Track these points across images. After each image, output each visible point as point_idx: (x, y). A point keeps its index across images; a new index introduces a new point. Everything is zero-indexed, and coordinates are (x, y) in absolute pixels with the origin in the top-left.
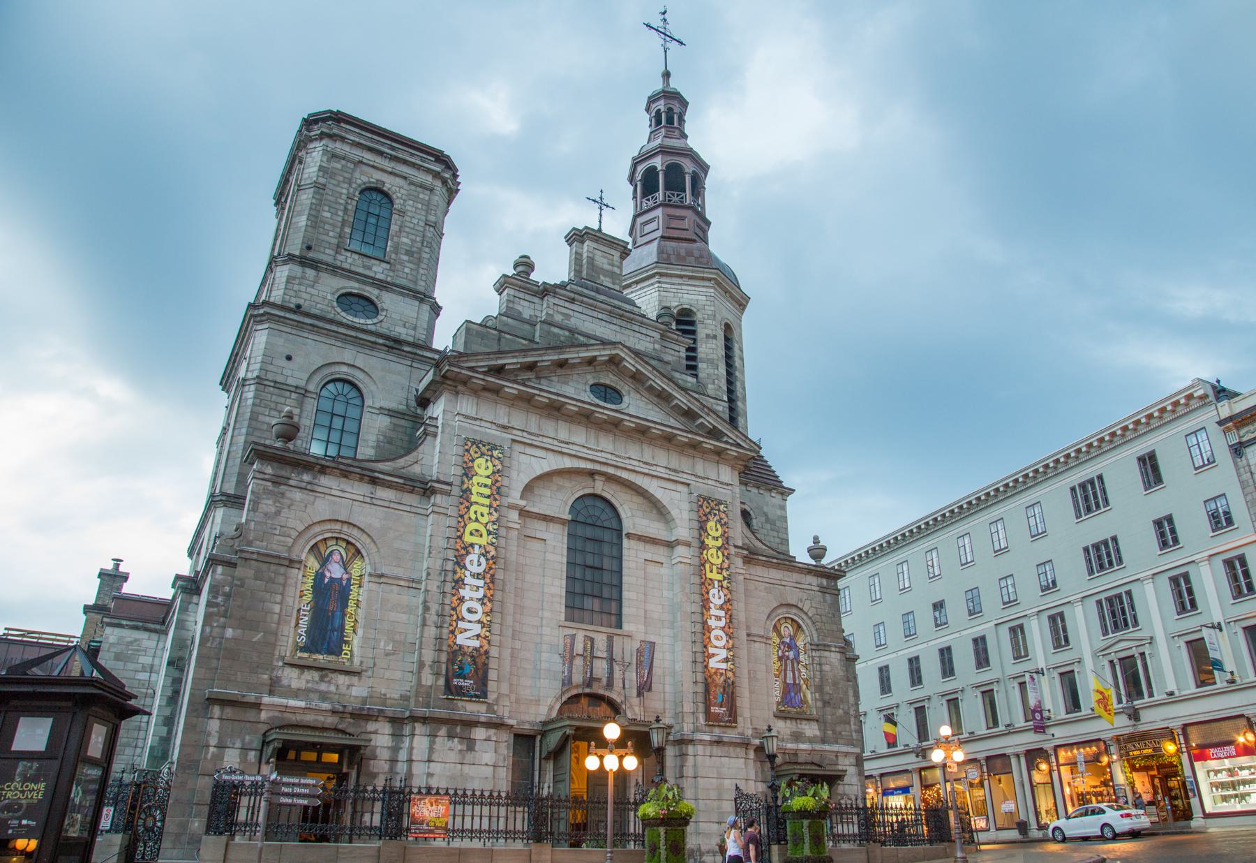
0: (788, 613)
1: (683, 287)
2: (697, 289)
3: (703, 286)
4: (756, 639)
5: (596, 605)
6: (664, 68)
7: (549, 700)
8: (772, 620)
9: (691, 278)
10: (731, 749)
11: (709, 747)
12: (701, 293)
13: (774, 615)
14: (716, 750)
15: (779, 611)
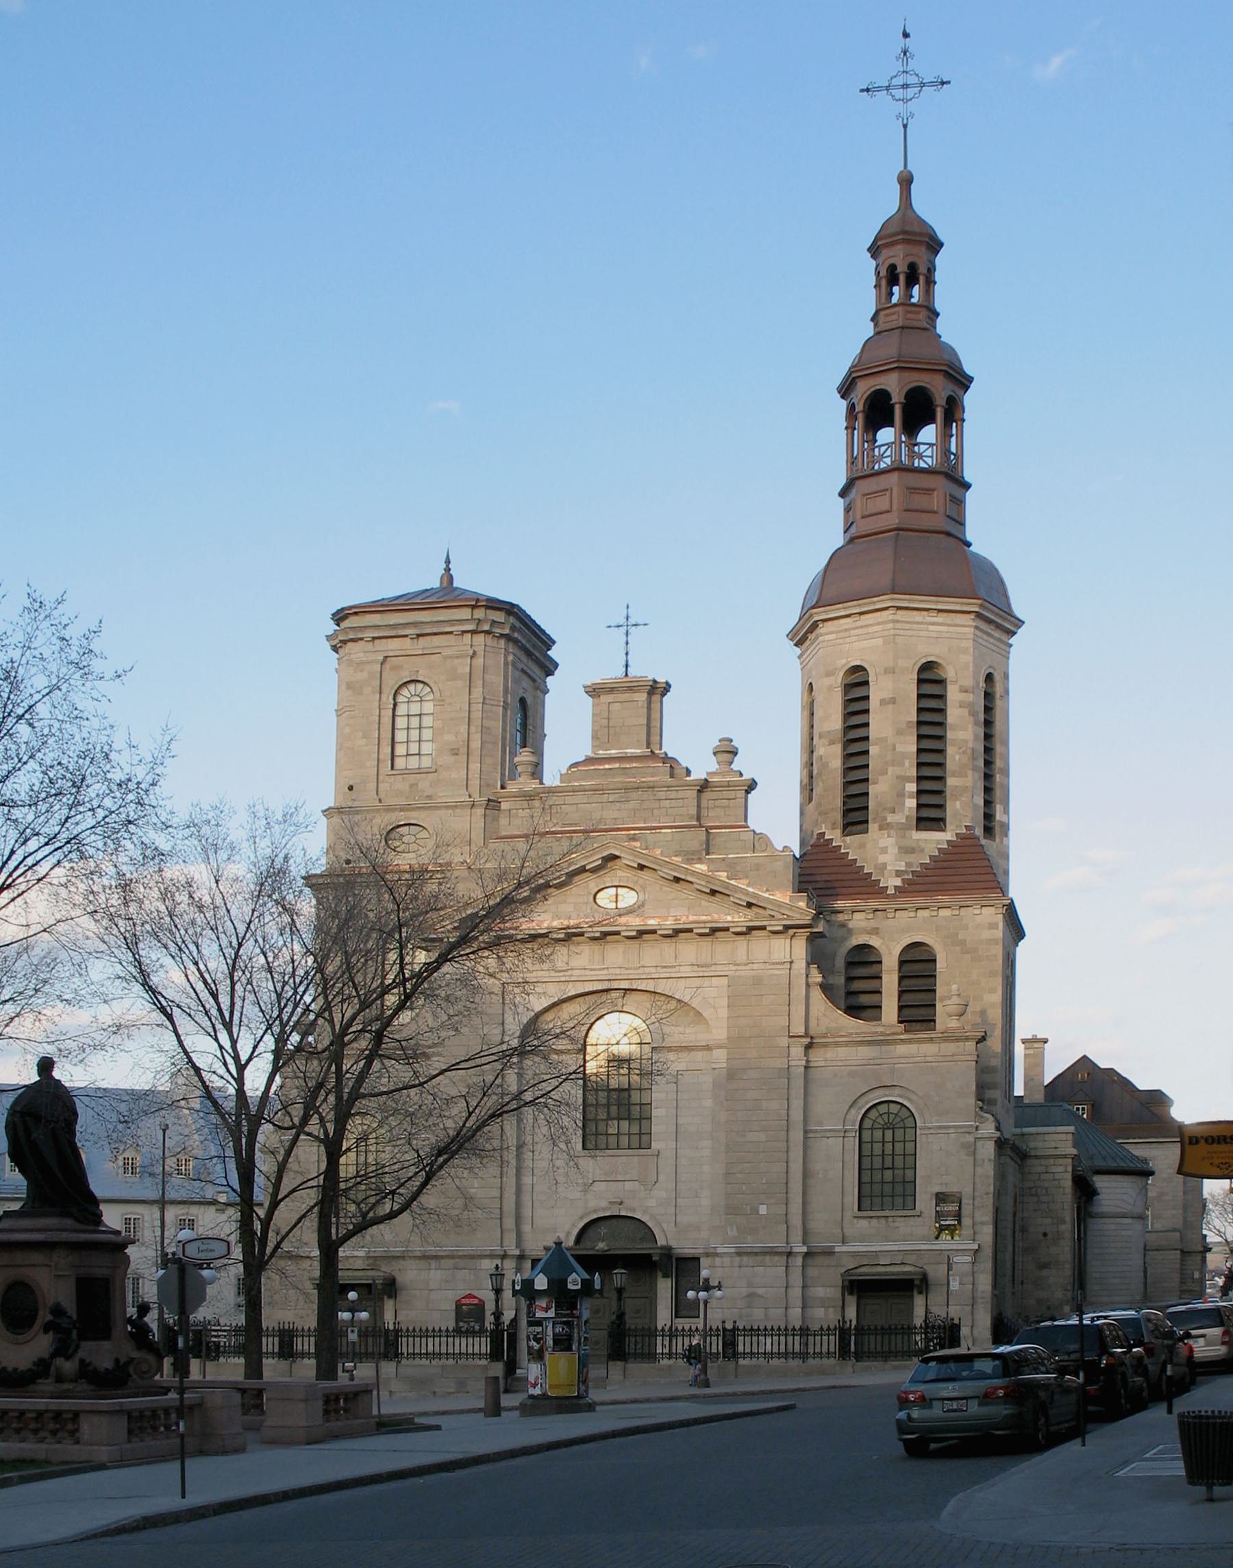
0: (887, 1096)
1: (852, 632)
2: (870, 630)
3: (878, 624)
4: (828, 1134)
5: (625, 1124)
6: (902, 168)
7: (567, 1227)
8: (860, 1108)
9: (861, 614)
10: (768, 1258)
11: (738, 1259)
12: (876, 634)
13: (862, 1101)
14: (745, 1259)
15: (871, 1095)
